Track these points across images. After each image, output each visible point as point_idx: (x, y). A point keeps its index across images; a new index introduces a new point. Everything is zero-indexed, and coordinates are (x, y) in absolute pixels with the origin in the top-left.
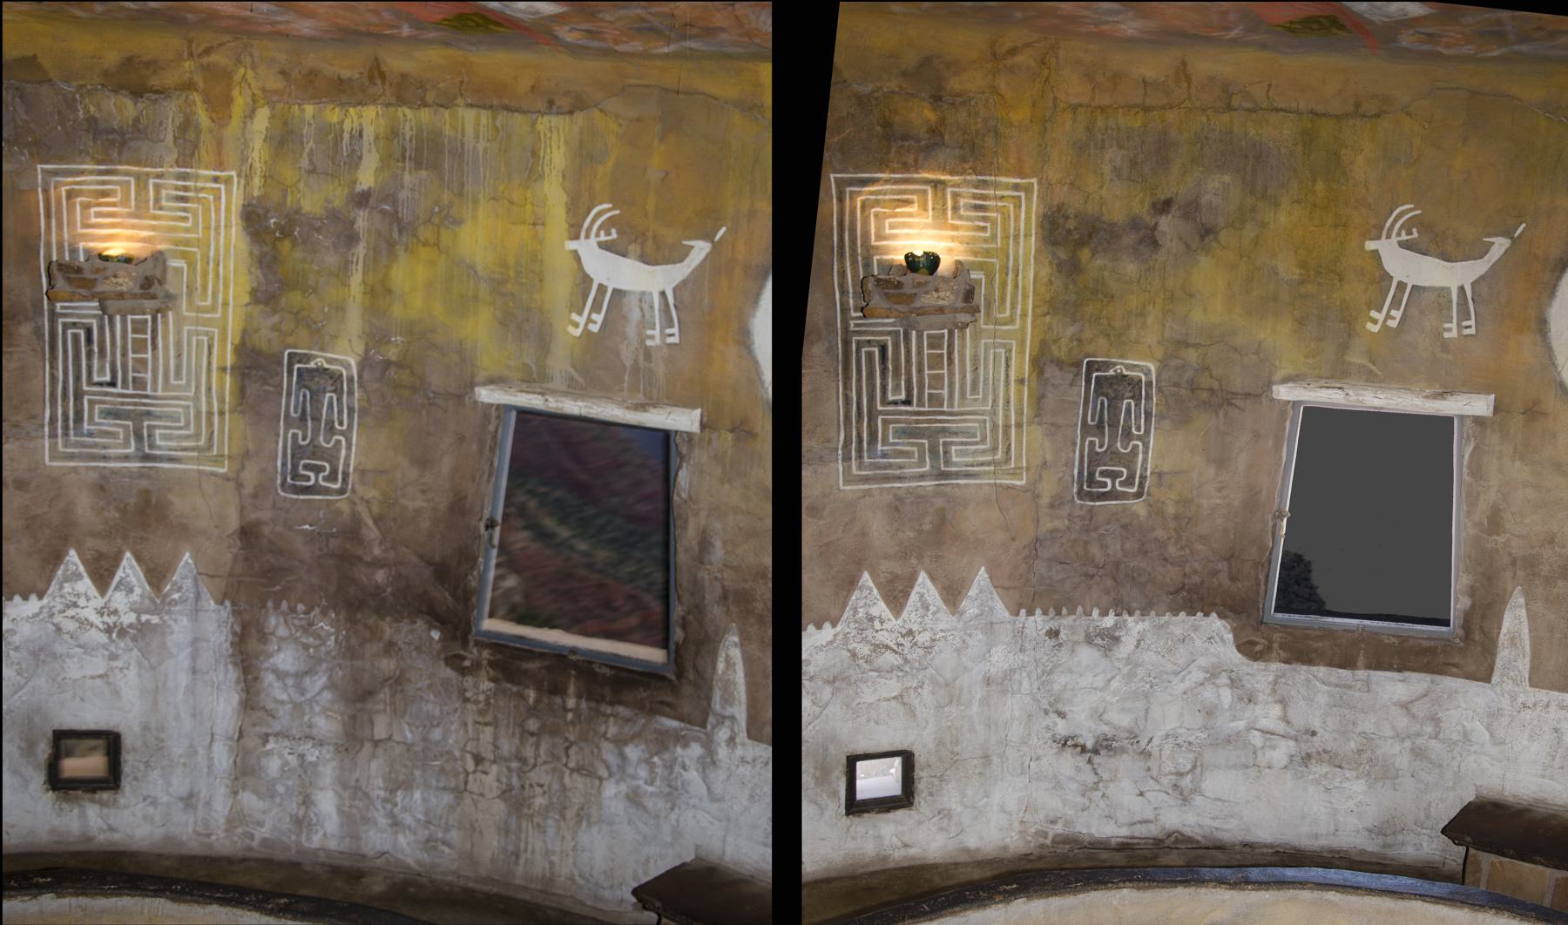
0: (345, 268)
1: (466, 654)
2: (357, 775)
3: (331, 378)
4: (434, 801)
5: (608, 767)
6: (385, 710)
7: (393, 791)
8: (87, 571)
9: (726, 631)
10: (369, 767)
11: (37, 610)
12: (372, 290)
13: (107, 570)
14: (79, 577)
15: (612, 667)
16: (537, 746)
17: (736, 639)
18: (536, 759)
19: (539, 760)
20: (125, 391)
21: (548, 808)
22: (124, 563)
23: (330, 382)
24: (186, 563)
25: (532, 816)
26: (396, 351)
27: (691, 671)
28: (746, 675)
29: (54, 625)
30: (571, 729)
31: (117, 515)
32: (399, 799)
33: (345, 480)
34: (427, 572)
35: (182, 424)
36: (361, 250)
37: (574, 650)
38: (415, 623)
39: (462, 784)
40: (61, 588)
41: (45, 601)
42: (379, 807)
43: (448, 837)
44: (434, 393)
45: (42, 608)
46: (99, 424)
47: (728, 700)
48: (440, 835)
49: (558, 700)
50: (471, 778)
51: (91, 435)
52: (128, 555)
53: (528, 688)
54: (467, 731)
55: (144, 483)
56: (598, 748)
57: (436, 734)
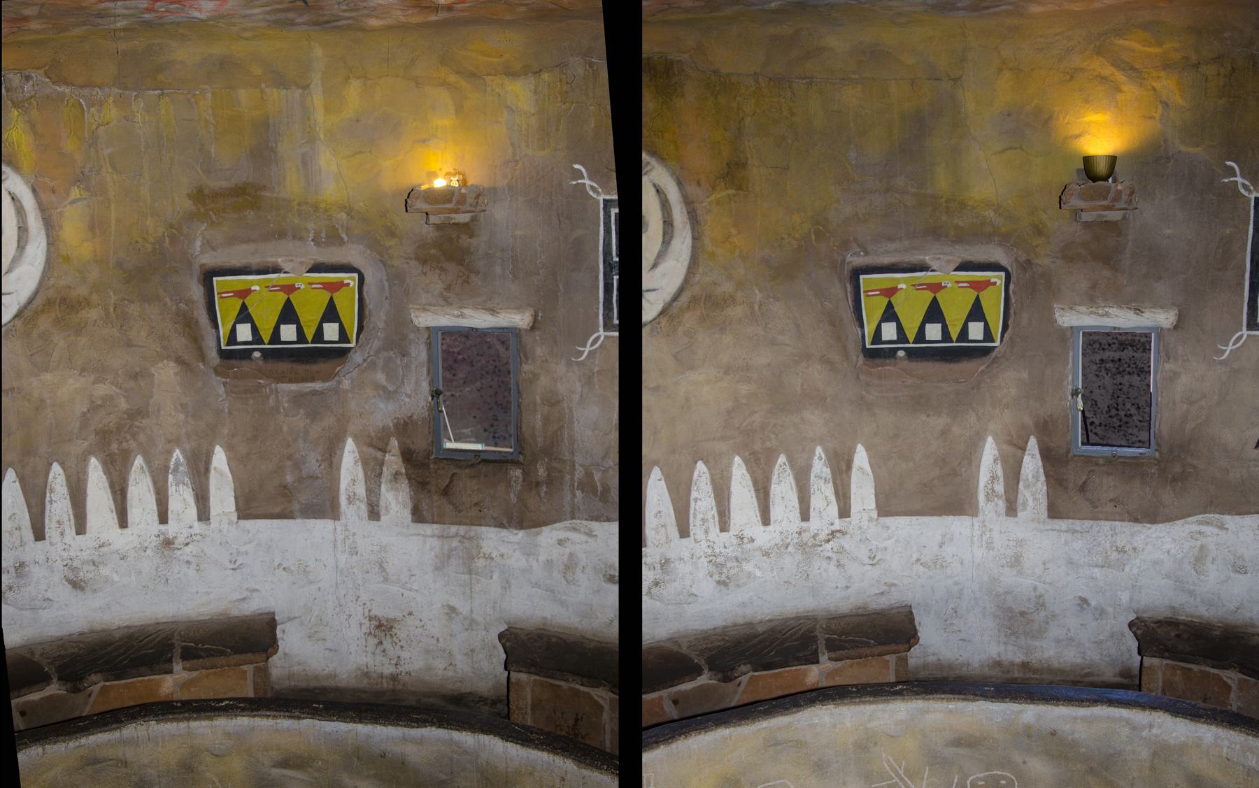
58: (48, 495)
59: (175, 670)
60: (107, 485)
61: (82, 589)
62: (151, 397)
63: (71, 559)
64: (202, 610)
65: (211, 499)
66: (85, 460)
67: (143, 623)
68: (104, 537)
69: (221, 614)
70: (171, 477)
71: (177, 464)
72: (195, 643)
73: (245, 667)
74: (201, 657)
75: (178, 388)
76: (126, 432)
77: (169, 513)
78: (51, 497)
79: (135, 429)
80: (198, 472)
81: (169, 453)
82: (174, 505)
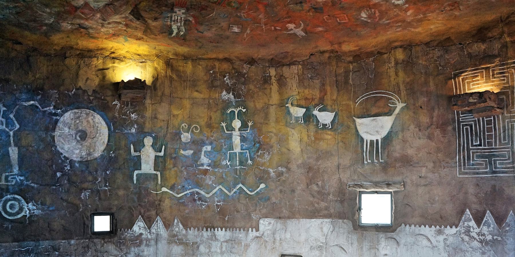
8: (473, 218)
11: (455, 232)
13: (480, 217)
14: (470, 220)
20: (485, 147)
22: (487, 215)
24: (511, 215)
29: (461, 238)
31: (483, 195)
35: (507, 158)
40: (464, 224)
41: (458, 229)
45: (457, 231)
46: (476, 161)
51: (473, 165)
52: (488, 211)
55: (493, 182)
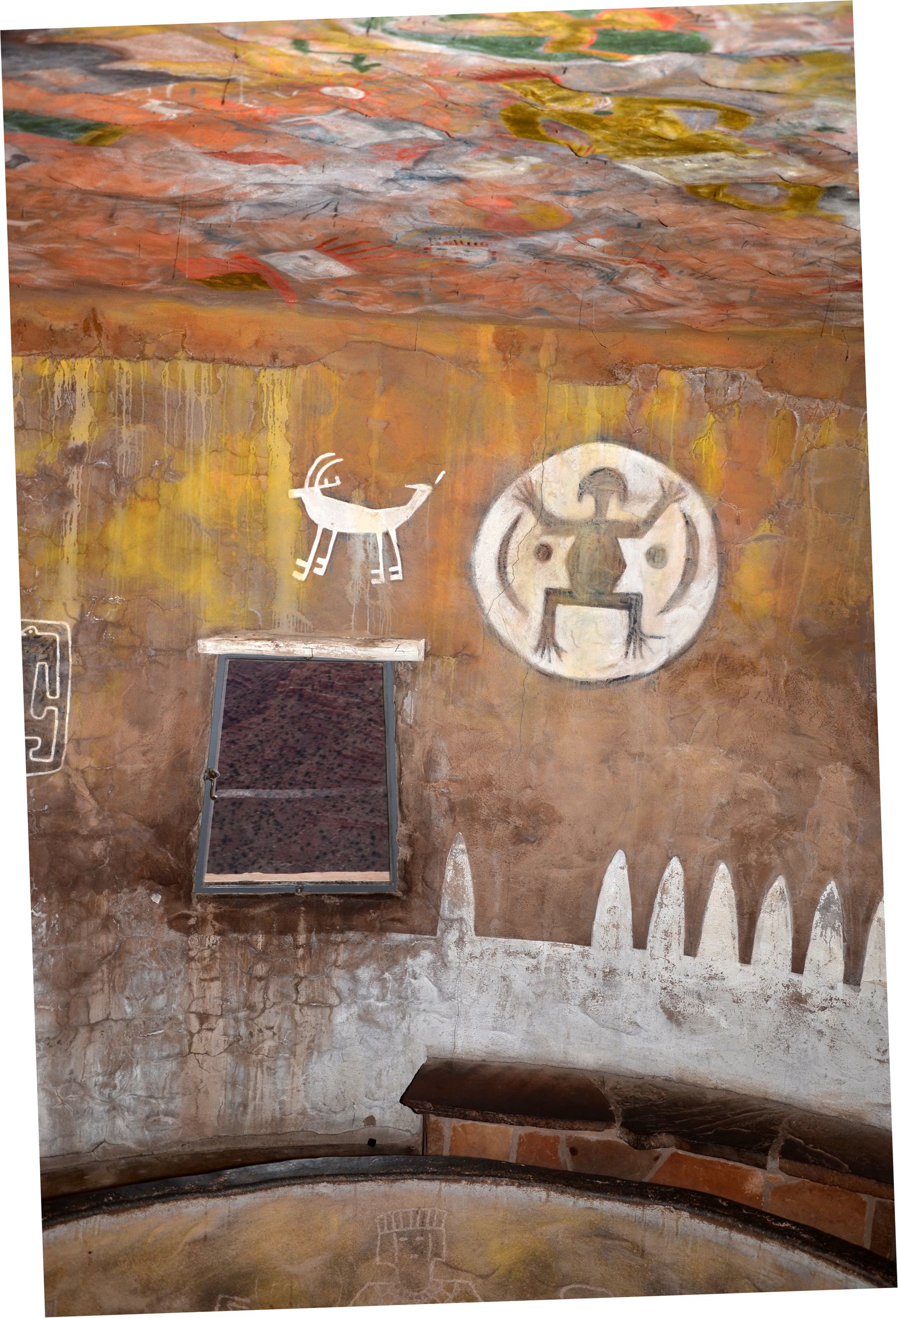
0: (59, 526)
1: (190, 912)
2: (72, 1066)
3: (43, 646)
4: (155, 1073)
5: (338, 994)
6: (102, 989)
7: (112, 1074)
9: (453, 840)
10: (85, 1054)
12: (87, 549)
15: (340, 896)
16: (266, 989)
17: (463, 846)
18: (265, 1004)
19: (268, 1003)
21: (277, 1050)
23: (41, 650)
25: (261, 1061)
26: (114, 610)
27: (420, 884)
28: (473, 878)
30: (301, 965)
32: (117, 1081)
33: (58, 753)
34: (148, 835)
36: (75, 508)
37: (300, 886)
38: (135, 890)
39: (187, 1047)
42: (96, 1095)
43: (172, 1106)
44: (155, 650)
47: (457, 904)
48: (163, 1106)
49: (289, 939)
50: (195, 1039)
53: (256, 933)
54: (192, 991)
56: (328, 977)
57: (160, 1001)
58: (659, 895)
59: (768, 1166)
60: (733, 902)
61: (679, 1024)
62: (811, 805)
63: (672, 983)
64: (828, 1101)
65: (867, 959)
66: (712, 864)
67: (747, 1092)
68: (718, 967)
69: (852, 1116)
70: (817, 916)
71: (830, 900)
72: (805, 1140)
73: (865, 1197)
74: (804, 1160)
75: (849, 802)
76: (770, 842)
77: (807, 961)
78: (662, 898)
79: (784, 842)
80: (856, 918)
81: (822, 884)
82: (815, 952)
